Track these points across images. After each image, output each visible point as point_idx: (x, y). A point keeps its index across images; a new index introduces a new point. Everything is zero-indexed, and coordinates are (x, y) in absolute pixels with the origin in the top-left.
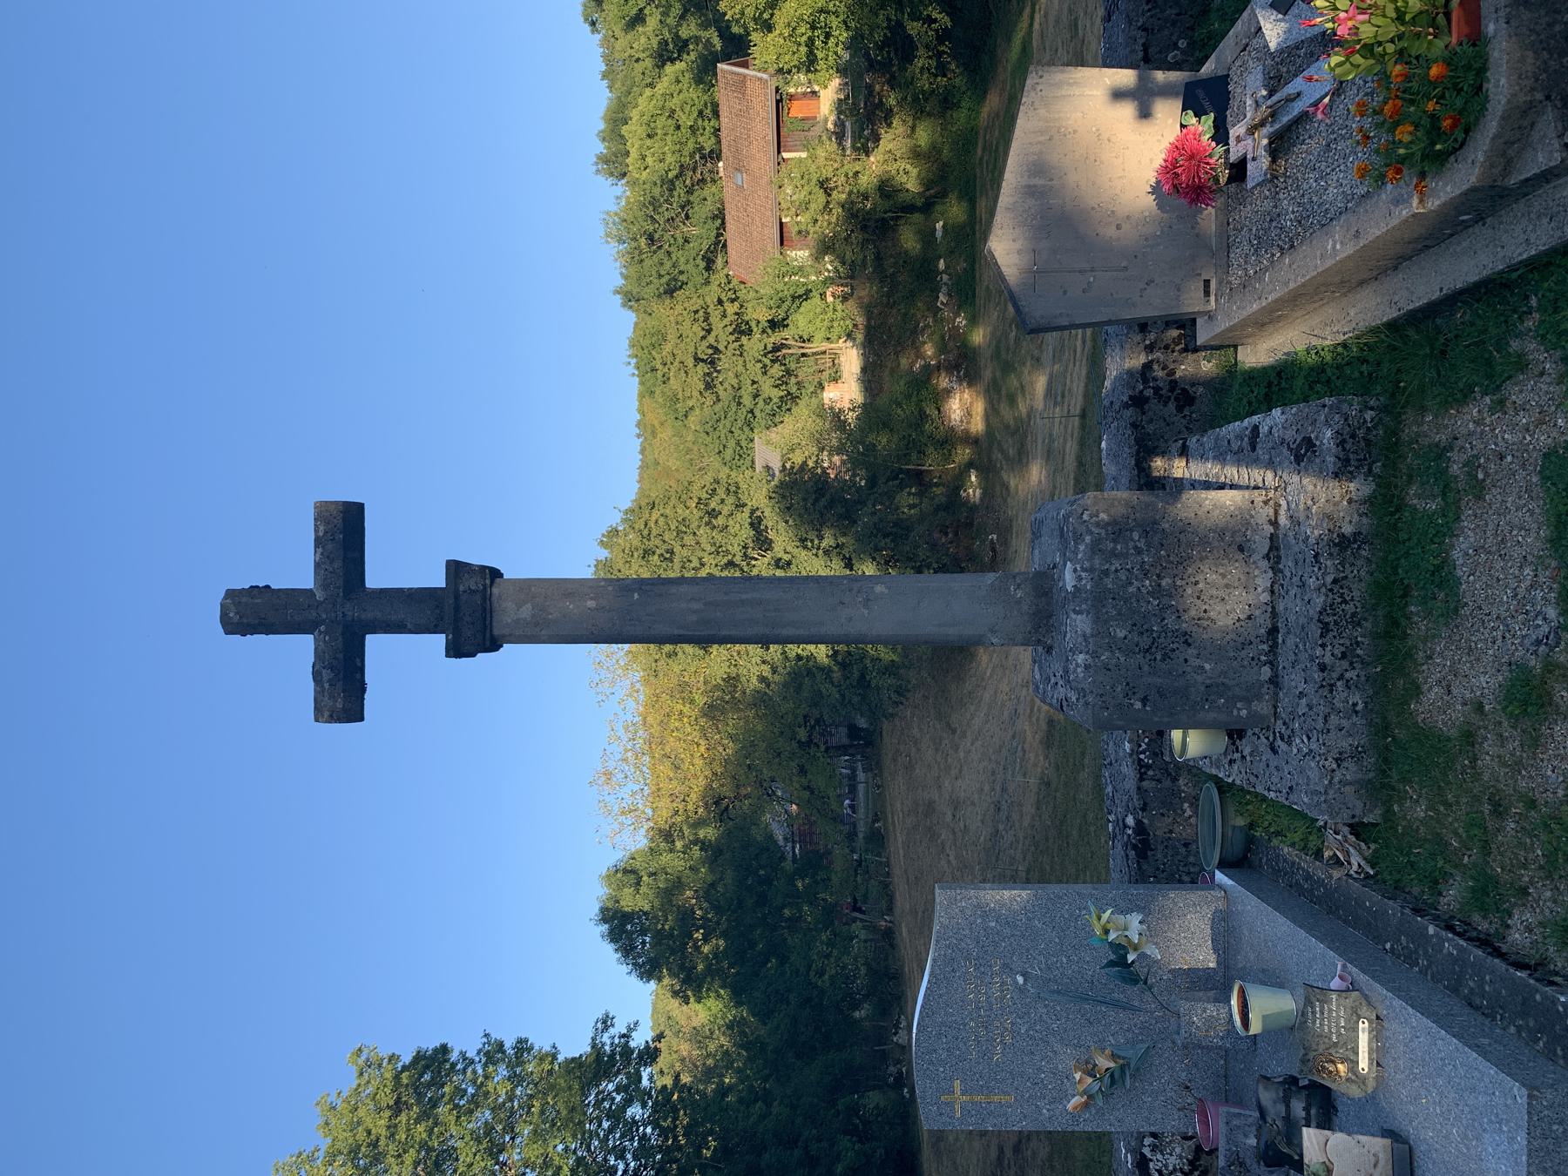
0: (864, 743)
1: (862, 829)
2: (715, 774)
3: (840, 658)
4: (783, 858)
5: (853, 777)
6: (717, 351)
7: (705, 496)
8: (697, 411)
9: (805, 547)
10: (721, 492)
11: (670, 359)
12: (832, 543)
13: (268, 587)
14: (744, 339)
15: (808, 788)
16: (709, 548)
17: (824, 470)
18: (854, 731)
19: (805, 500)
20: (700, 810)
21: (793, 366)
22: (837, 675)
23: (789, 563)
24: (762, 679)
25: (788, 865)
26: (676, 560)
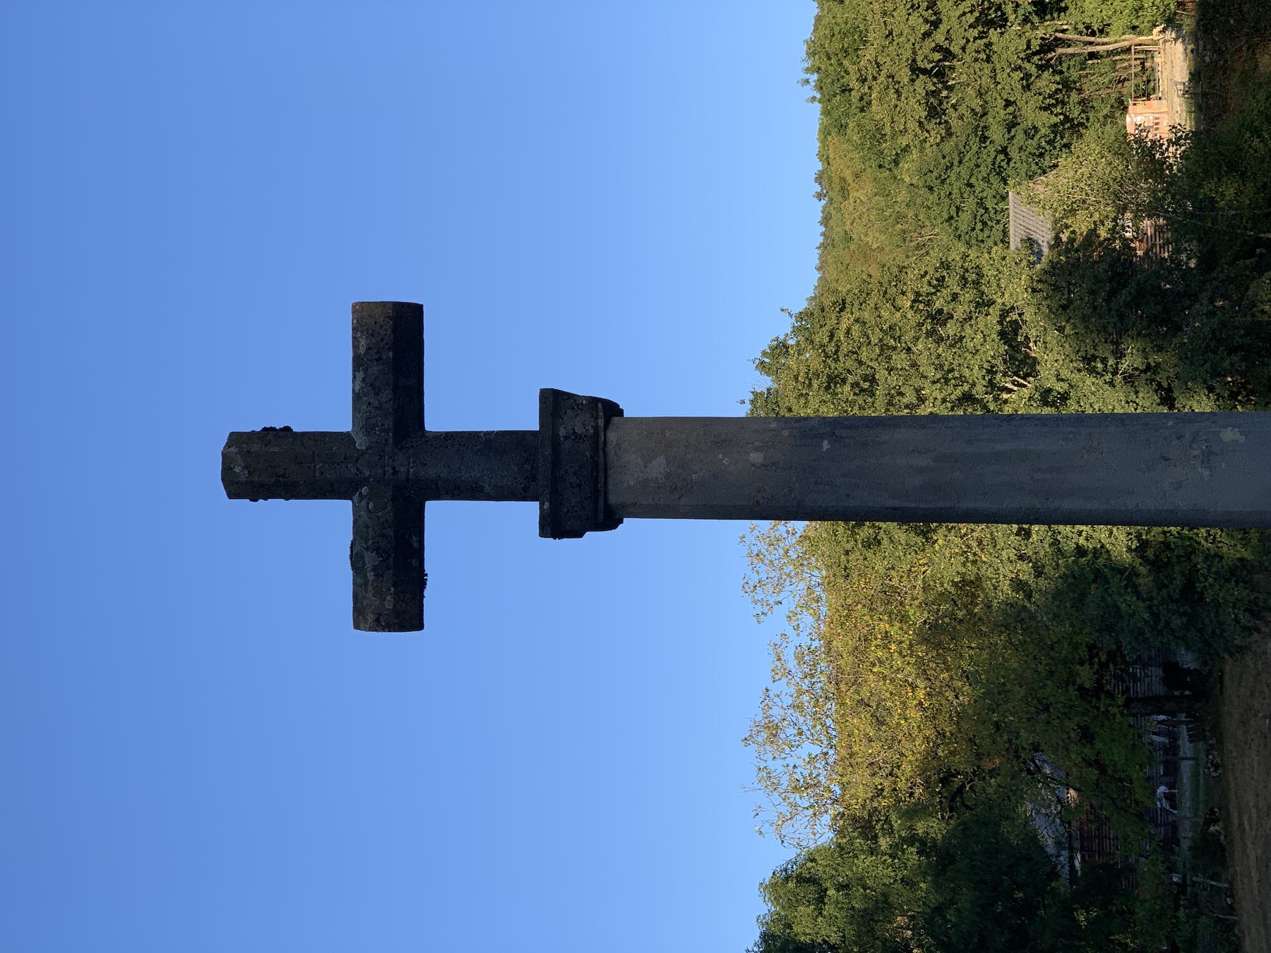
0: (1194, 696)
1: (1187, 834)
2: (941, 734)
3: (1150, 553)
4: (1054, 874)
5: (1172, 749)
6: (948, 54)
7: (926, 289)
8: (915, 154)
9: (1092, 371)
10: (953, 284)
11: (872, 71)
12: (1139, 362)
13: (287, 429)
14: (993, 34)
15: (1097, 763)
16: (931, 372)
17: (1125, 241)
18: (1173, 674)
19: (1092, 292)
20: (918, 791)
21: (1074, 74)
22: (1145, 581)
23: (1064, 397)
24: (1018, 585)
25: (1062, 886)
26: (880, 392)
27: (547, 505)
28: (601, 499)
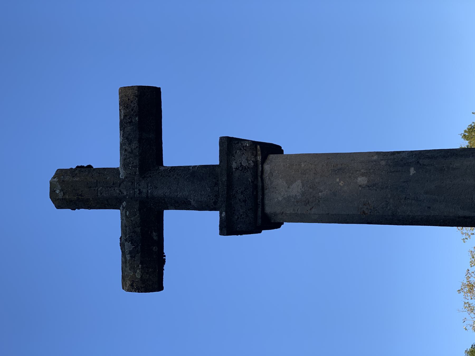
13: (90, 167)
27: (224, 214)
28: (260, 210)
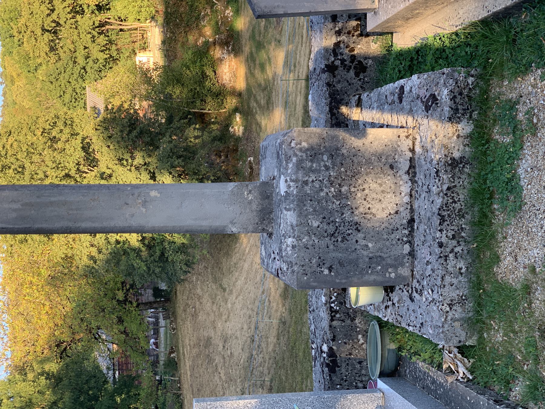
0: (164, 300)
1: (162, 359)
2: (56, 325)
3: (146, 242)
4: (106, 382)
5: (156, 323)
6: (58, 24)
7: (48, 127)
8: (44, 67)
9: (122, 165)
10: (60, 124)
11: (24, 29)
12: (141, 162)
14: (78, 17)
15: (125, 332)
16: (50, 164)
17: (136, 111)
18: (157, 292)
19: (121, 131)
20: (46, 352)
21: (114, 37)
22: (145, 253)
23: (110, 176)
24: (92, 258)
25: (110, 386)
26: (27, 173)
